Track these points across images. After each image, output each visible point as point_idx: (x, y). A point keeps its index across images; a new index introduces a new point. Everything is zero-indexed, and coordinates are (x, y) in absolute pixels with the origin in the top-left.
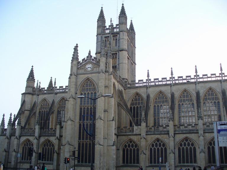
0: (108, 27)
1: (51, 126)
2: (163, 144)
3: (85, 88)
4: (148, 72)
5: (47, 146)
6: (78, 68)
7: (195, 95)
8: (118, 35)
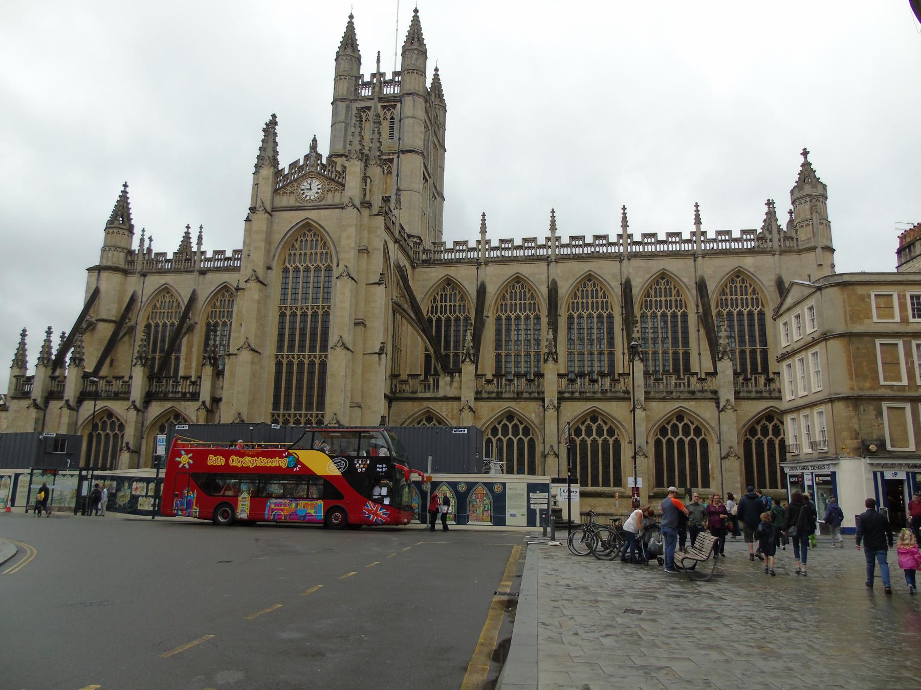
0: (367, 79)
1: (185, 369)
2: (523, 429)
3: (298, 253)
4: (484, 220)
6: (276, 191)
7: (618, 291)
8: (399, 105)
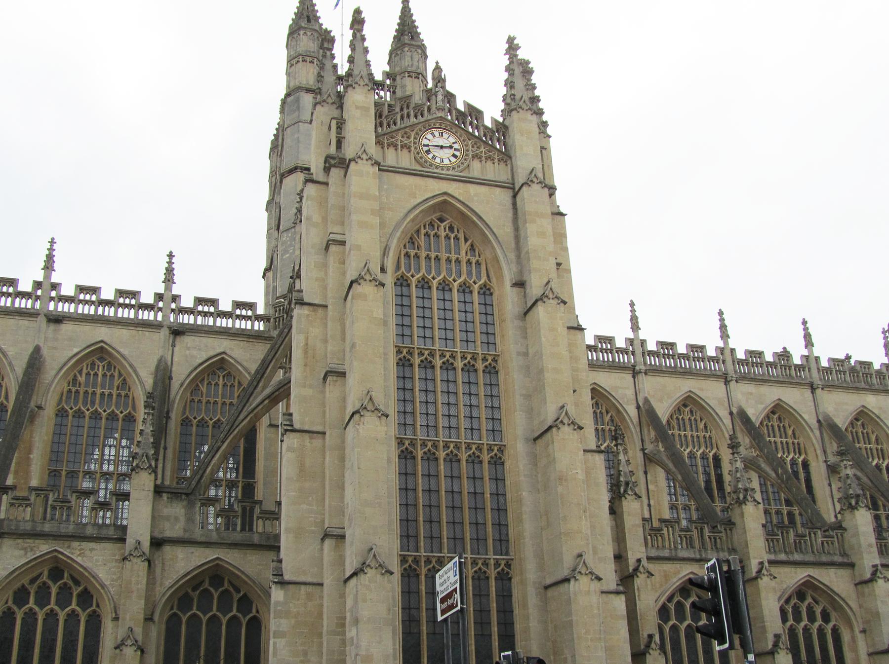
5: (43, 598)
